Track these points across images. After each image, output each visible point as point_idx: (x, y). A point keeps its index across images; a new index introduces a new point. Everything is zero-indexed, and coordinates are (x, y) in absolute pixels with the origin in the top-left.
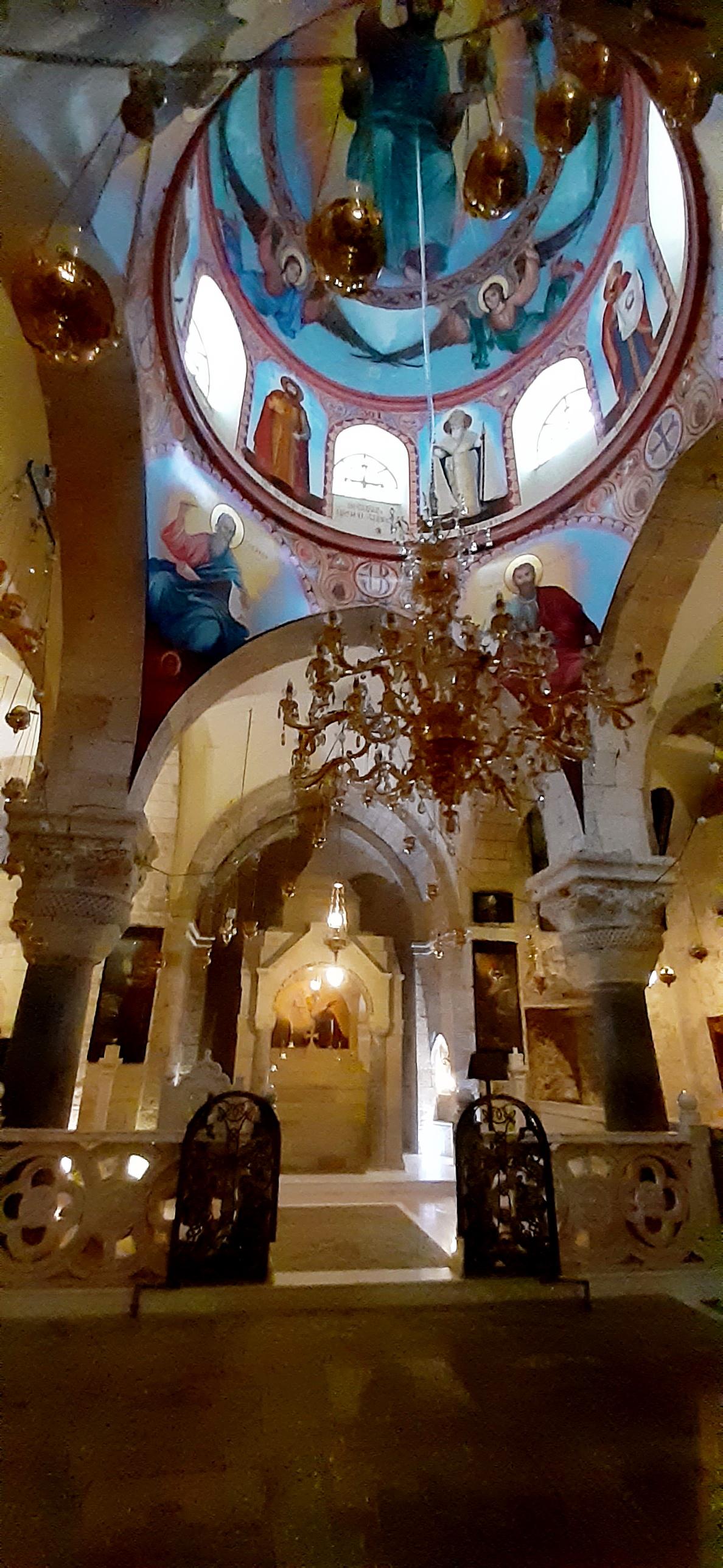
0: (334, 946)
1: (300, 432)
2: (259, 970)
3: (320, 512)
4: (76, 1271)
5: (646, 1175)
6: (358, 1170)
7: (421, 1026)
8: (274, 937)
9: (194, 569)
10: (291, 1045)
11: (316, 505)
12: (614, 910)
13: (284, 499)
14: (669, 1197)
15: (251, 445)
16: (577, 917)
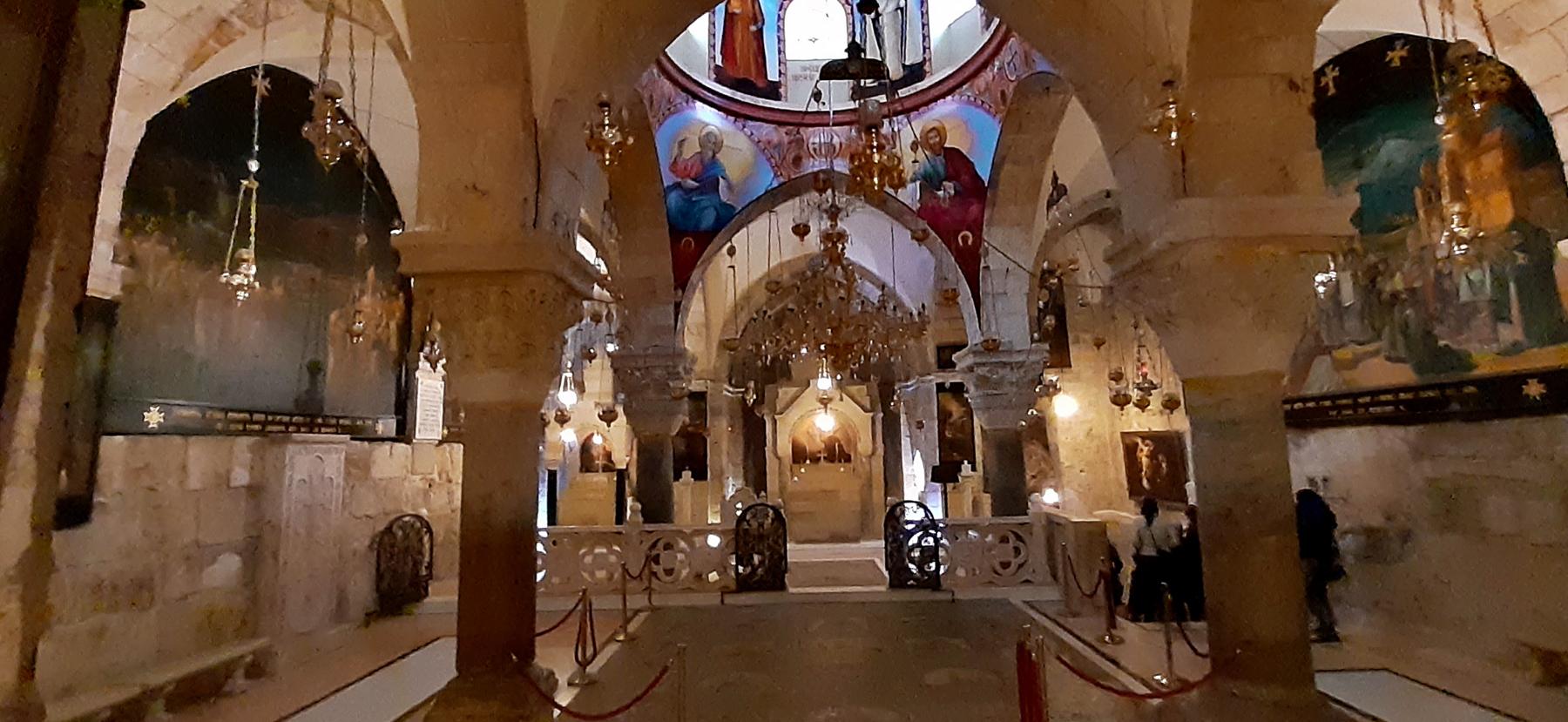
0: (825, 402)
1: (756, 23)
2: (776, 417)
3: (777, 97)
4: (693, 586)
5: (1004, 540)
6: (856, 540)
7: (905, 443)
8: (785, 392)
9: (693, 180)
10: (808, 462)
11: (773, 91)
12: (999, 383)
13: (749, 99)
14: (1017, 551)
15: (719, 62)
16: (977, 387)
